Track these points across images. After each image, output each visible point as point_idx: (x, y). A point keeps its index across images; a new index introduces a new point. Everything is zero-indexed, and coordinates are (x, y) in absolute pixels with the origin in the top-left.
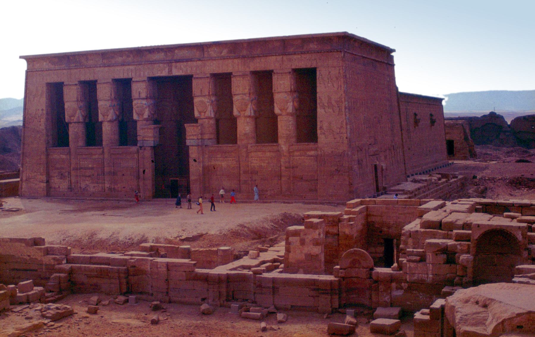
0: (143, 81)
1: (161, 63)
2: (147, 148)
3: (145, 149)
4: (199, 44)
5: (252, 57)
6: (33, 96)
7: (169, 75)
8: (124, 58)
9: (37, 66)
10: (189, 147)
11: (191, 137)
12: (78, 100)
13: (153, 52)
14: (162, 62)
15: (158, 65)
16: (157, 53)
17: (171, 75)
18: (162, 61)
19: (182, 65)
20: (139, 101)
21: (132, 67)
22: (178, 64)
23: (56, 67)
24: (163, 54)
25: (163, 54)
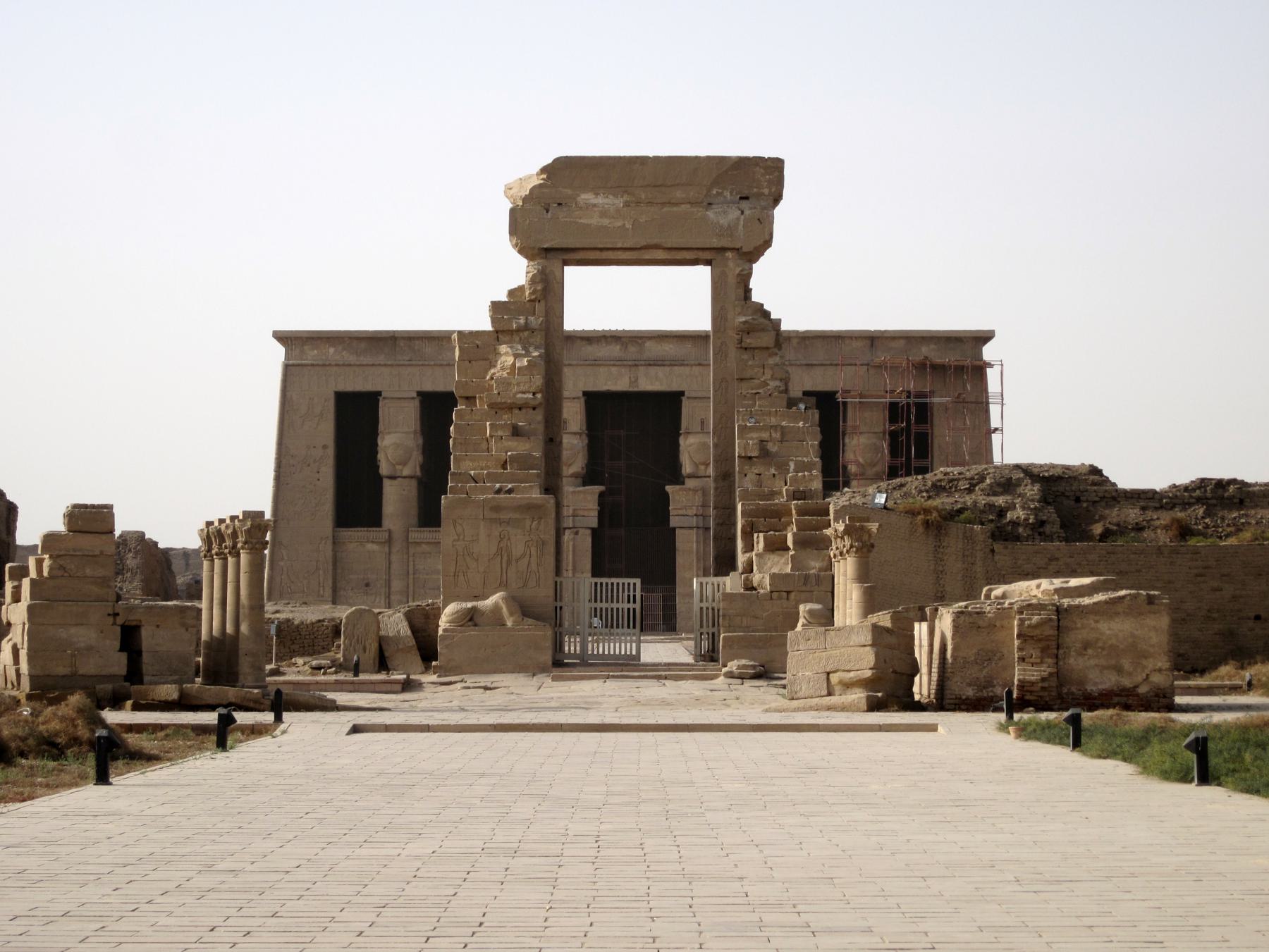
0: (574, 398)
1: (614, 365)
2: (581, 531)
3: (577, 533)
4: (703, 334)
6: (302, 417)
7: (631, 389)
11: (680, 512)
12: (415, 432)
13: (598, 341)
15: (606, 369)
16: (604, 345)
17: (636, 389)
18: (618, 362)
19: (661, 372)
22: (653, 370)
23: (362, 358)
24: (618, 347)
25: (618, 347)
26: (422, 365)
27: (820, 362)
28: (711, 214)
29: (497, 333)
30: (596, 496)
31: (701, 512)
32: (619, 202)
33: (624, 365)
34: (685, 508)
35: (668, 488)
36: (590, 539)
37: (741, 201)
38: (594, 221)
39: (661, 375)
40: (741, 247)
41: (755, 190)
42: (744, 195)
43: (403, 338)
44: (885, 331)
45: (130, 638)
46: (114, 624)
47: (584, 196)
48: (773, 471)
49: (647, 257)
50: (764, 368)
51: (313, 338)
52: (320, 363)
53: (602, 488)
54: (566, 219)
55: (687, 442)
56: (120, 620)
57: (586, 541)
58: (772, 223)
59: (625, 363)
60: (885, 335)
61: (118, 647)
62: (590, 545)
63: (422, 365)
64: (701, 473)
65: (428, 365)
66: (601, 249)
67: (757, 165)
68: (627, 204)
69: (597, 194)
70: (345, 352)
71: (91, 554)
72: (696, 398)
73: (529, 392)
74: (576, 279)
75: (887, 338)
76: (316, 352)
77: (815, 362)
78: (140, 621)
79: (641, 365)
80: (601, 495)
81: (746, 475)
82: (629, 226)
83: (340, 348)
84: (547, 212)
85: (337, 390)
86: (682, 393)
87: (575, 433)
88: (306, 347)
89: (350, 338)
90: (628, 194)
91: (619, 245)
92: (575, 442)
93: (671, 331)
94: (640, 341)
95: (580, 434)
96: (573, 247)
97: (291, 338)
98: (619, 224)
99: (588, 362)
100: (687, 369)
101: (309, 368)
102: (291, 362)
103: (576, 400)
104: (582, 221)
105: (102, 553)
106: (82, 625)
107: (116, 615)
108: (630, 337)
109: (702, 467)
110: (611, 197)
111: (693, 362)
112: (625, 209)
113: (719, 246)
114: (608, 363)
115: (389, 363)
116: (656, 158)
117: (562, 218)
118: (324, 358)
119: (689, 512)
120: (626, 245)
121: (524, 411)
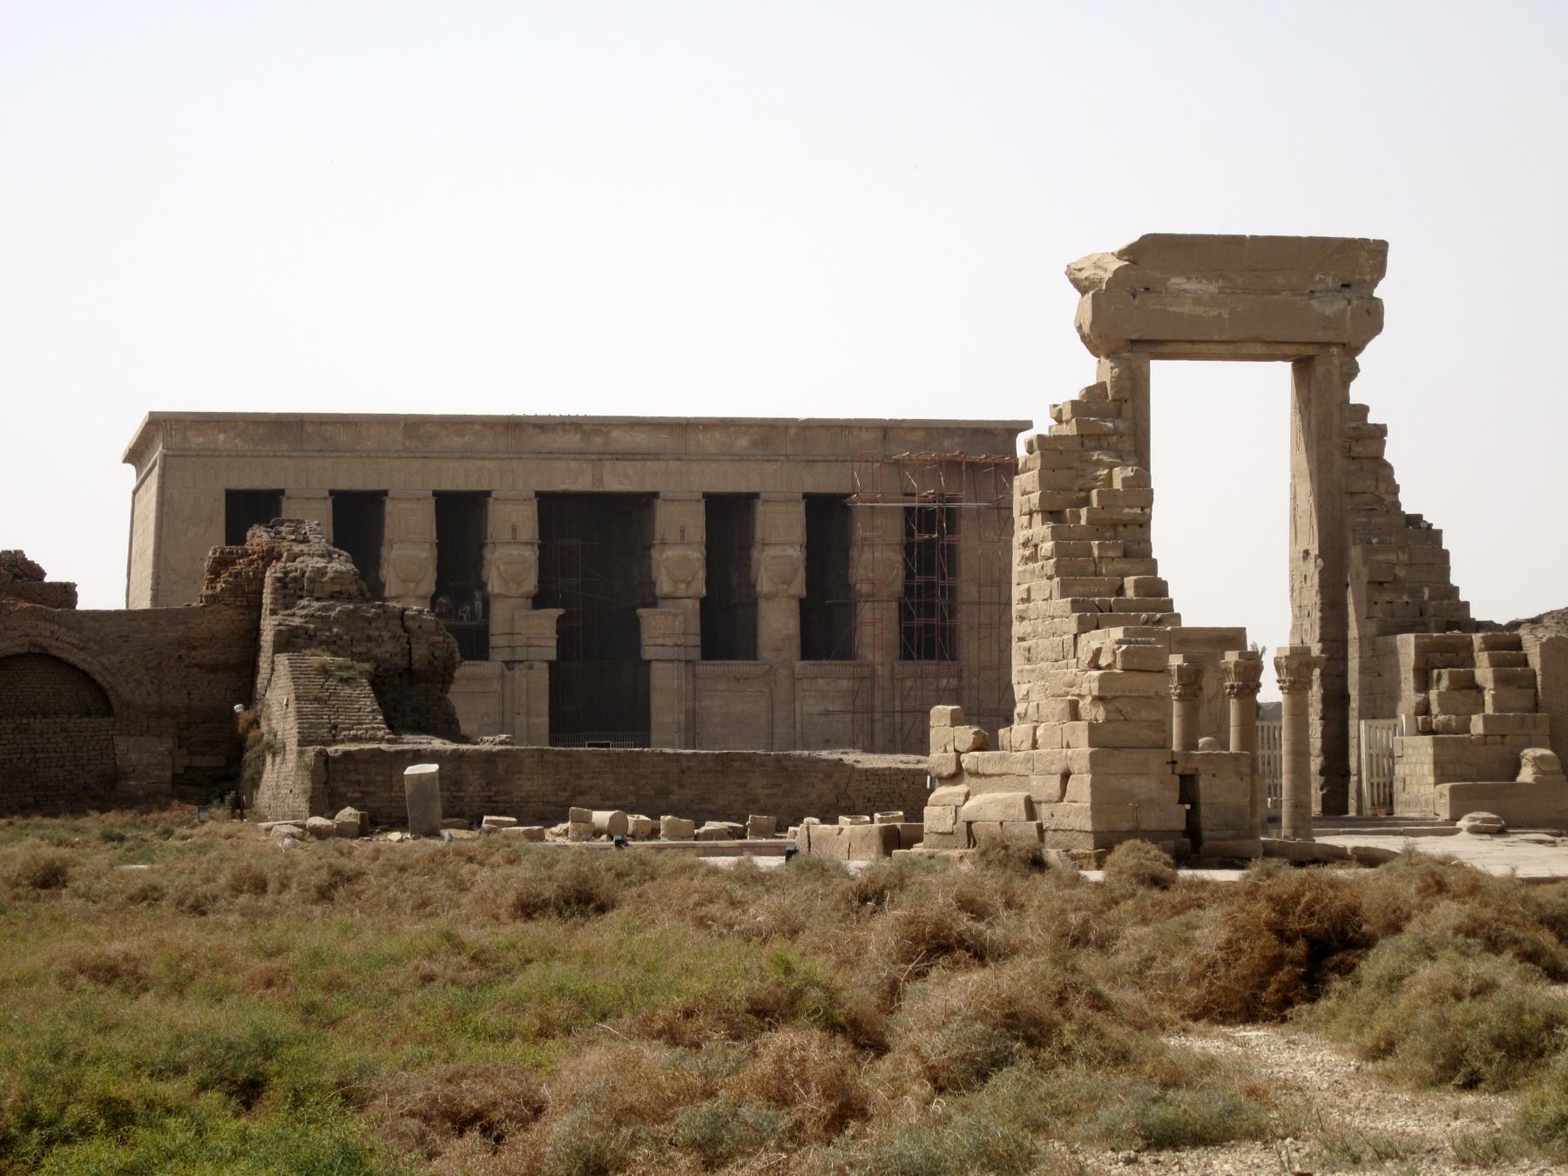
2: (537, 665)
3: (531, 668)
5: (809, 461)
7: (595, 489)
8: (466, 439)
9: (197, 441)
10: (654, 665)
11: (658, 641)
13: (554, 429)
14: (579, 457)
16: (561, 434)
17: (600, 489)
18: (579, 454)
19: (630, 467)
20: (515, 552)
21: (488, 464)
22: (620, 465)
24: (578, 437)
25: (578, 437)
26: (337, 457)
27: (823, 458)
28: (1315, 304)
29: (1082, 436)
30: (555, 621)
31: (681, 640)
32: (1212, 288)
33: (585, 460)
34: (664, 635)
35: (642, 612)
36: (547, 676)
37: (1343, 289)
38: (1187, 309)
39: (630, 471)
40: (1349, 343)
41: (1357, 277)
42: (1345, 283)
43: (313, 423)
44: (903, 421)
45: (1188, 787)
46: (1173, 773)
47: (1174, 280)
48: (1405, 598)
49: (1244, 351)
50: (1377, 481)
51: (198, 422)
52: (208, 453)
53: (561, 611)
54: (1155, 307)
55: (664, 555)
56: (1178, 770)
57: (542, 677)
58: (1382, 314)
59: (587, 456)
60: (903, 425)
61: (1177, 799)
62: (547, 682)
63: (337, 457)
64: (682, 593)
65: (344, 457)
66: (1193, 342)
67: (1362, 248)
68: (1222, 291)
69: (1189, 278)
70: (237, 441)
71: (1146, 694)
72: (673, 500)
73: (1137, 507)
74: (1166, 377)
75: (903, 428)
76: (201, 439)
77: (817, 458)
78: (1197, 770)
79: (608, 459)
80: (560, 619)
81: (1376, 603)
82: (1225, 316)
83: (232, 434)
84: (1134, 297)
85: (228, 487)
86: (655, 495)
87: (527, 544)
88: (189, 433)
89: (246, 422)
90: (1224, 278)
91: (1216, 338)
92: (527, 554)
93: (644, 418)
94: (605, 430)
95: (532, 544)
96: (1164, 338)
97: (170, 421)
98: (1214, 313)
99: (541, 456)
100: (663, 464)
101: (194, 459)
102: (171, 453)
103: (527, 502)
104: (1173, 309)
105: (1157, 693)
106: (1143, 774)
107: (1174, 763)
108: (593, 425)
109: (683, 586)
110: (1204, 281)
111: (670, 456)
112: (1221, 296)
113: (1326, 340)
114: (567, 456)
115: (295, 454)
116: (1254, 238)
117: (1153, 304)
118: (212, 446)
119: (669, 641)
120: (1225, 338)
121: (1130, 527)
